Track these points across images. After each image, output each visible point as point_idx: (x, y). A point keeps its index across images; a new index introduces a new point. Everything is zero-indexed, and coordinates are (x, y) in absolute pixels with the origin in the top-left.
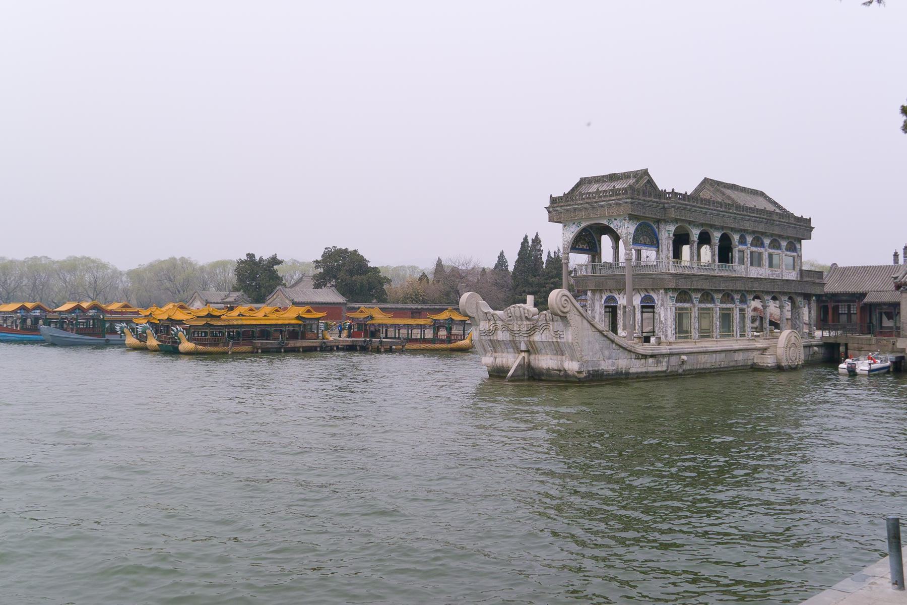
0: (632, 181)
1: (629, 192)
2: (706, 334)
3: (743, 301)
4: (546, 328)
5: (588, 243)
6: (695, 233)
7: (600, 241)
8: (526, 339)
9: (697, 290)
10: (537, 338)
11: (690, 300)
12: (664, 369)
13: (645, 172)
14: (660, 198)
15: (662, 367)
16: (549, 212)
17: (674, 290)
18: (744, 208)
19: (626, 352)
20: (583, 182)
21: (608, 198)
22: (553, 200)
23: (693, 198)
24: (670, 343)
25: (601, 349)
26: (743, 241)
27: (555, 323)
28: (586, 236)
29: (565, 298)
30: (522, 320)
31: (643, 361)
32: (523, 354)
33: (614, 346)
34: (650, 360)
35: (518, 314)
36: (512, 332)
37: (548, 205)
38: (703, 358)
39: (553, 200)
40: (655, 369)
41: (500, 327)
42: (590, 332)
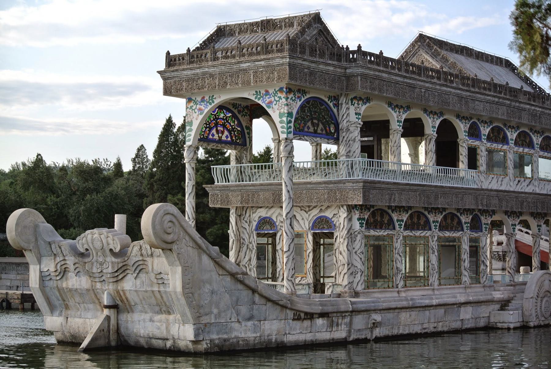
0: (293, 31)
1: (287, 47)
2: (413, 278)
3: (476, 226)
4: (140, 269)
5: (229, 131)
6: (396, 119)
7: (250, 128)
8: (111, 287)
9: (399, 209)
10: (129, 284)
11: (390, 224)
13: (317, 18)
14: (339, 60)
15: (340, 334)
16: (164, 79)
17: (362, 208)
18: (476, 82)
19: (279, 308)
20: (221, 32)
21: (254, 58)
22: (171, 60)
23: (401, 64)
24: (356, 294)
26: (474, 133)
27: (156, 260)
28: (226, 119)
29: (168, 217)
30: (104, 256)
31: (307, 323)
32: (106, 312)
34: (320, 322)
35: (98, 245)
36: (91, 275)
37: (162, 67)
39: (171, 60)
41: (72, 267)
42: (215, 276)
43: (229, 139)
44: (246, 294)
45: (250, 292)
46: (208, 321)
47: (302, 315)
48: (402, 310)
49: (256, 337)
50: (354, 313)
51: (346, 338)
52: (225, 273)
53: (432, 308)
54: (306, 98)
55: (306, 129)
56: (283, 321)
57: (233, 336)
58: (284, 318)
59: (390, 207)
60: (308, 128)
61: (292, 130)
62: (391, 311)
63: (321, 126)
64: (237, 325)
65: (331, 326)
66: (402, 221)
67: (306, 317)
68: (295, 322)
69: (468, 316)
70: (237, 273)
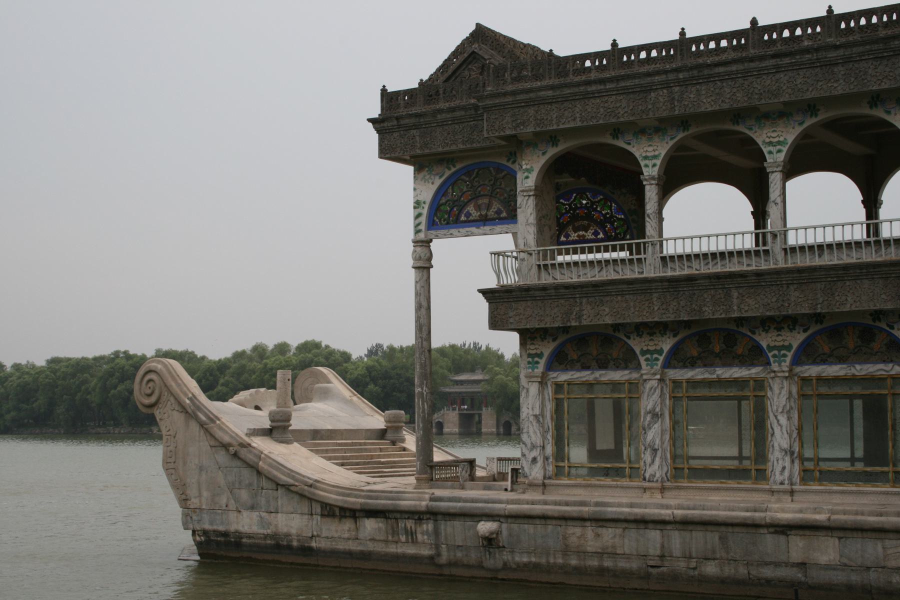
11: (629, 360)
12: (426, 552)
13: (481, 34)
19: (296, 498)
25: (231, 489)
31: (348, 524)
33: (265, 483)
34: (370, 525)
38: (591, 540)
40: (392, 549)
43: (601, 236)
44: (247, 475)
45: (255, 473)
46: (197, 506)
47: (337, 512)
48: (570, 523)
49: (266, 537)
50: (439, 517)
51: (431, 558)
52: (217, 444)
53: (669, 527)
54: (453, 170)
55: (463, 218)
56: (306, 517)
57: (232, 528)
58: (306, 511)
59: (616, 327)
60: (468, 215)
61: (422, 227)
62: (538, 521)
63: (496, 205)
64: (235, 514)
65: (395, 532)
66: (660, 352)
67: (343, 514)
68: (324, 520)
69: (823, 559)
70: (230, 445)
